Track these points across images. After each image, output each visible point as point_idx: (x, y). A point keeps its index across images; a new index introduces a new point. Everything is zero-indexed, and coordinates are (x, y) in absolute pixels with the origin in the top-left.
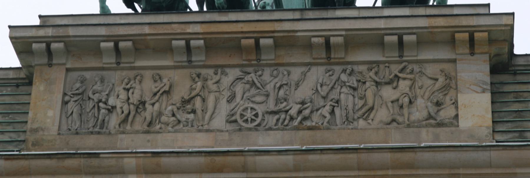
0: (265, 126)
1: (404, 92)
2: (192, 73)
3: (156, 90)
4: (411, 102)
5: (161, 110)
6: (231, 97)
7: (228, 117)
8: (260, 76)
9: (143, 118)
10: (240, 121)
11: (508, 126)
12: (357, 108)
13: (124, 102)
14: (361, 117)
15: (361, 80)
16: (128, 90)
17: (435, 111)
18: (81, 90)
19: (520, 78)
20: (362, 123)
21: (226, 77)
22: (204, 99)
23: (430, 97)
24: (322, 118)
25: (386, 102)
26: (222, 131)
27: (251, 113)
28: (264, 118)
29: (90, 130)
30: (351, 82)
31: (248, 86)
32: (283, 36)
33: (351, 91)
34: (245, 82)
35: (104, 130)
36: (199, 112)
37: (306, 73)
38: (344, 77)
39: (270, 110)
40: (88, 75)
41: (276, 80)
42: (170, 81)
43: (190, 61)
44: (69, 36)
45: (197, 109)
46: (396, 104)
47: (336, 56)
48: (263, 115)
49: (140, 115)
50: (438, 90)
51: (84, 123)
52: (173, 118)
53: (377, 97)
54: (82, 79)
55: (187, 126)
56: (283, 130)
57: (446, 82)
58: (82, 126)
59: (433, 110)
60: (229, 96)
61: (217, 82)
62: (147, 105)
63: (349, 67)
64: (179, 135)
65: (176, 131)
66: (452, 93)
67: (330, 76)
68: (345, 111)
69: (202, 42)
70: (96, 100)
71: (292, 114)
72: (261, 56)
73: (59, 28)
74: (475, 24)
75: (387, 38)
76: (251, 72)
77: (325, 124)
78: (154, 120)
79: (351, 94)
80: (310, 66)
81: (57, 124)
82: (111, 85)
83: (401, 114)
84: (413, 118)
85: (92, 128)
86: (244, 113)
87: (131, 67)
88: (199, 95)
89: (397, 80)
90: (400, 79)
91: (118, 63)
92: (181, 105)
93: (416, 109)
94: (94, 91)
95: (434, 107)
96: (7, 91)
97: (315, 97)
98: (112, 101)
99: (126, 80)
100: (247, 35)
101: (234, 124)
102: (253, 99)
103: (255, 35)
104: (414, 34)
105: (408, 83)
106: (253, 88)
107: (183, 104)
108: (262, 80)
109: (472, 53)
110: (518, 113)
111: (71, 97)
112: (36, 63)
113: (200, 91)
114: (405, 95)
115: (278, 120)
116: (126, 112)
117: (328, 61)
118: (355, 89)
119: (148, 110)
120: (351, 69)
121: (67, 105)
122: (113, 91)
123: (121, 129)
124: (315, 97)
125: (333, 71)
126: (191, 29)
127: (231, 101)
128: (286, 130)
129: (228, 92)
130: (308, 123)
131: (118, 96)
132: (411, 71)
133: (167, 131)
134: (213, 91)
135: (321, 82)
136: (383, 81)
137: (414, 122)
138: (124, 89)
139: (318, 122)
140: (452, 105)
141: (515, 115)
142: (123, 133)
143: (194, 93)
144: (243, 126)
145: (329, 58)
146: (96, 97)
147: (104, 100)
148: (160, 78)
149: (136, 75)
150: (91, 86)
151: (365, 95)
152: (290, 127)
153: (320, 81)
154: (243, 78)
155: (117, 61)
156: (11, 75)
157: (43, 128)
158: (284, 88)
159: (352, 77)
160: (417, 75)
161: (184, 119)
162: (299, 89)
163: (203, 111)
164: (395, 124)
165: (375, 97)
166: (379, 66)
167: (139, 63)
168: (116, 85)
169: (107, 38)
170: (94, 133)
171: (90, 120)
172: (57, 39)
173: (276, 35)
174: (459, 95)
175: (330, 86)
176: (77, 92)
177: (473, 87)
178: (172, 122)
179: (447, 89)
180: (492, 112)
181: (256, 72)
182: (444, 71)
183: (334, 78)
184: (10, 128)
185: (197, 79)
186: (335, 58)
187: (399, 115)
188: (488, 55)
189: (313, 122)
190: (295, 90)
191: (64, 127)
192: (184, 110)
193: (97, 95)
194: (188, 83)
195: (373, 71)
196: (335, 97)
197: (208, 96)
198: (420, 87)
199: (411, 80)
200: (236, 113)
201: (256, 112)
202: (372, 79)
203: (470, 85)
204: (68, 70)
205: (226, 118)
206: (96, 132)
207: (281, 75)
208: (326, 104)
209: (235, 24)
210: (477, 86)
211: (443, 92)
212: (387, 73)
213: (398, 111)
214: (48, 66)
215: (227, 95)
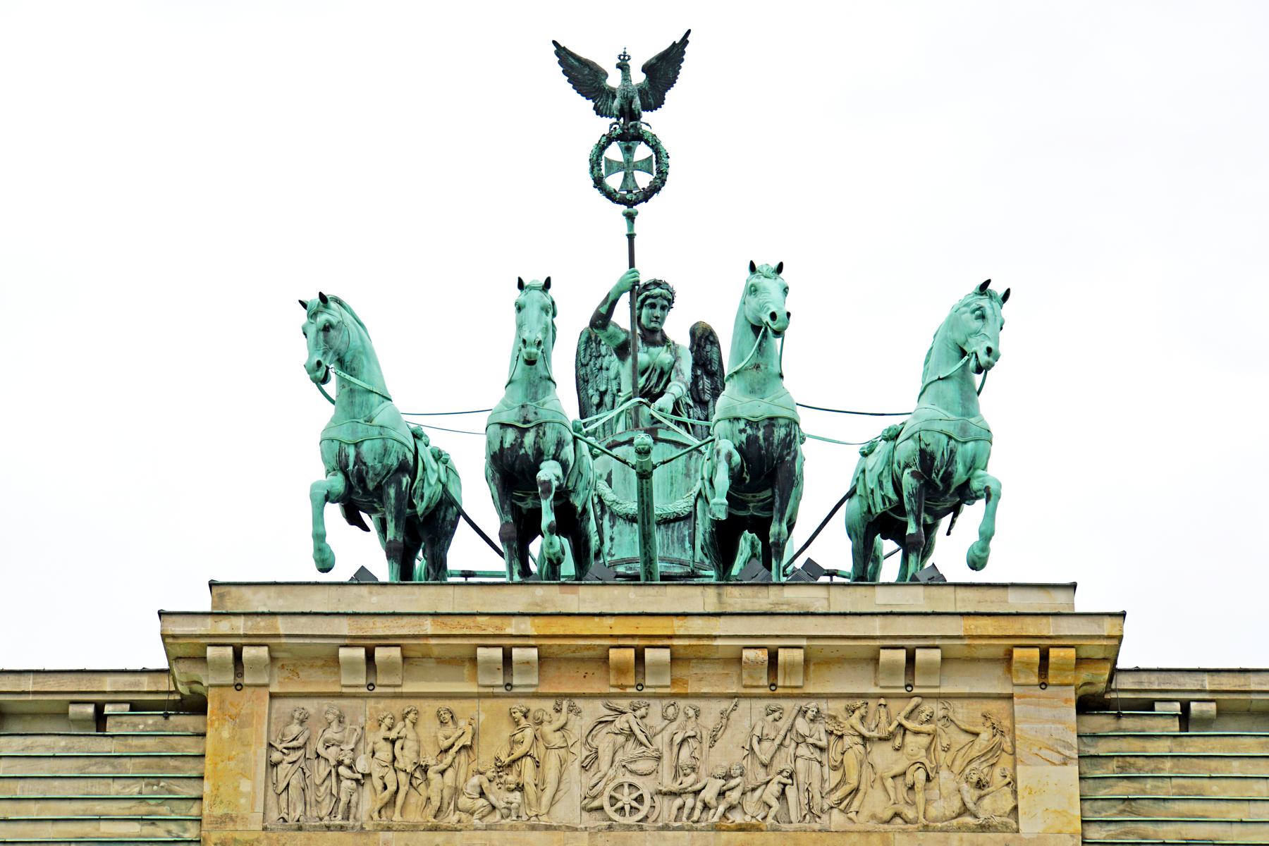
0: (655, 821)
1: (915, 759)
2: (514, 710)
3: (447, 743)
4: (928, 779)
5: (458, 784)
6: (588, 760)
7: (587, 800)
8: (643, 717)
9: (423, 798)
10: (609, 810)
11: (1110, 831)
12: (827, 787)
13: (386, 766)
14: (836, 806)
15: (835, 732)
16: (393, 742)
17: (975, 799)
18: (301, 741)
19: (1128, 724)
20: (837, 818)
21: (578, 718)
22: (538, 762)
23: (963, 770)
24: (762, 806)
25: (882, 778)
26: (576, 830)
27: (630, 794)
28: (654, 805)
29: (326, 822)
30: (816, 736)
31: (621, 739)
32: (690, 646)
33: (817, 754)
34: (617, 732)
35: (351, 822)
36: (530, 789)
37: (729, 714)
38: (802, 726)
39: (664, 790)
40: (311, 706)
41: (675, 725)
42: (474, 725)
43: (509, 685)
44: (278, 636)
45: (528, 783)
46: (900, 780)
47: (787, 684)
48: (652, 798)
49: (416, 790)
50: (979, 757)
51: (311, 807)
52: (482, 802)
53: (864, 767)
54: (302, 716)
55: (507, 817)
56: (691, 829)
57: (994, 742)
58: (308, 813)
59: (970, 794)
60: (586, 758)
61: (562, 728)
62: (430, 774)
63: (812, 705)
64: (495, 835)
65: (489, 828)
66: (1005, 761)
67: (775, 720)
68: (806, 794)
69: (535, 652)
70: (333, 762)
71: (707, 800)
72: (644, 678)
73: (259, 619)
74: (1051, 634)
75: (885, 655)
76: (626, 711)
77: (770, 820)
78: (445, 805)
79: (818, 761)
80: (736, 699)
81: (260, 809)
82: (359, 730)
83: (910, 802)
84: (933, 812)
85: (327, 818)
86: (617, 795)
87: (395, 693)
88: (530, 756)
89: (902, 732)
90: (907, 732)
91: (371, 686)
92: (494, 774)
93: (938, 792)
94: (326, 741)
95: (972, 790)
96: (146, 725)
97: (747, 763)
98: (361, 766)
99: (388, 721)
100: (621, 642)
101: (597, 815)
102: (632, 767)
103: (636, 642)
104: (936, 647)
105: (924, 740)
106: (632, 740)
107: (498, 772)
108: (646, 726)
109: (1043, 683)
110: (1126, 803)
111: (284, 753)
112: (212, 682)
113: (530, 749)
114: (918, 765)
115: (681, 808)
116: (392, 788)
117: (771, 692)
118: (822, 749)
119: (432, 783)
120: (816, 710)
121: (275, 768)
122: (363, 741)
123: (384, 821)
124: (747, 763)
125: (781, 711)
126: (513, 627)
127: (591, 766)
128: (696, 830)
129: (583, 748)
130: (737, 817)
131: (374, 753)
132: (928, 718)
133: (472, 828)
134: (556, 747)
135: (759, 734)
136: (875, 734)
137: (935, 821)
138: (386, 739)
139: (754, 815)
140: (1006, 788)
141: (1121, 806)
142: (389, 829)
143: (518, 751)
144: (616, 821)
145: (773, 685)
146: (332, 754)
147: (347, 761)
148: (452, 717)
149: (406, 711)
150: (321, 731)
151: (842, 760)
152: (703, 824)
153: (757, 732)
154: (612, 721)
155: (369, 682)
156: (146, 683)
157: (234, 815)
158: (690, 744)
159: (817, 725)
160: (940, 724)
161: (503, 805)
162: (716, 744)
163: (536, 785)
164: (899, 820)
165: (861, 767)
166: (867, 704)
167: (408, 688)
168: (367, 728)
169: (352, 641)
170: (332, 829)
171: (323, 800)
172: (256, 640)
173: (675, 642)
174: (1018, 767)
175: (777, 742)
176: (295, 744)
177: (1045, 753)
178: (480, 808)
179: (996, 753)
180: (1081, 800)
181: (634, 710)
182: (990, 718)
183: (784, 725)
184: (164, 811)
185: (523, 722)
186: (784, 687)
187: (907, 803)
188: (1073, 688)
189: (745, 813)
190: (710, 747)
191: (274, 815)
192: (501, 783)
193: (333, 750)
194: (507, 730)
195: (857, 713)
196: (788, 767)
197: (545, 753)
198: (946, 749)
199: (929, 734)
200: (601, 793)
201: (639, 793)
202: (856, 731)
203: (1040, 748)
204: (273, 696)
205: (581, 802)
206: (336, 826)
207: (681, 718)
208: (771, 780)
209: (597, 619)
210: (1053, 750)
211: (988, 759)
212: (884, 718)
213: (905, 796)
214: (234, 687)
215: (581, 753)
